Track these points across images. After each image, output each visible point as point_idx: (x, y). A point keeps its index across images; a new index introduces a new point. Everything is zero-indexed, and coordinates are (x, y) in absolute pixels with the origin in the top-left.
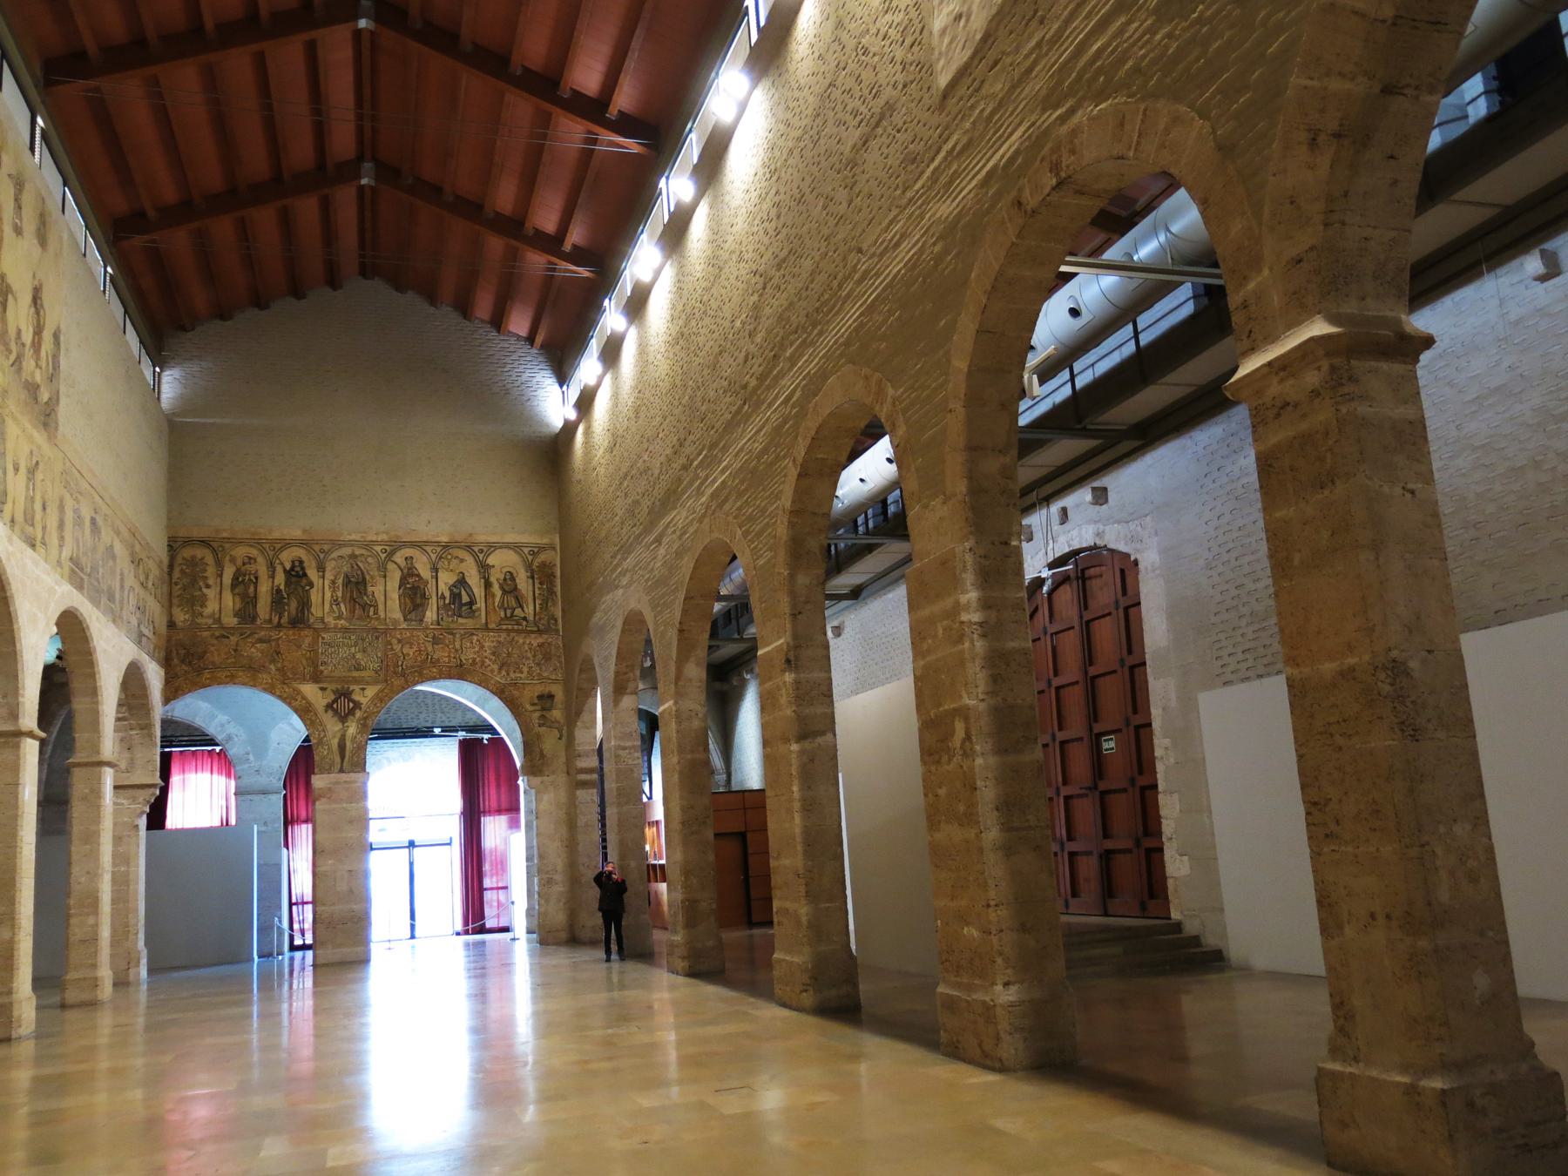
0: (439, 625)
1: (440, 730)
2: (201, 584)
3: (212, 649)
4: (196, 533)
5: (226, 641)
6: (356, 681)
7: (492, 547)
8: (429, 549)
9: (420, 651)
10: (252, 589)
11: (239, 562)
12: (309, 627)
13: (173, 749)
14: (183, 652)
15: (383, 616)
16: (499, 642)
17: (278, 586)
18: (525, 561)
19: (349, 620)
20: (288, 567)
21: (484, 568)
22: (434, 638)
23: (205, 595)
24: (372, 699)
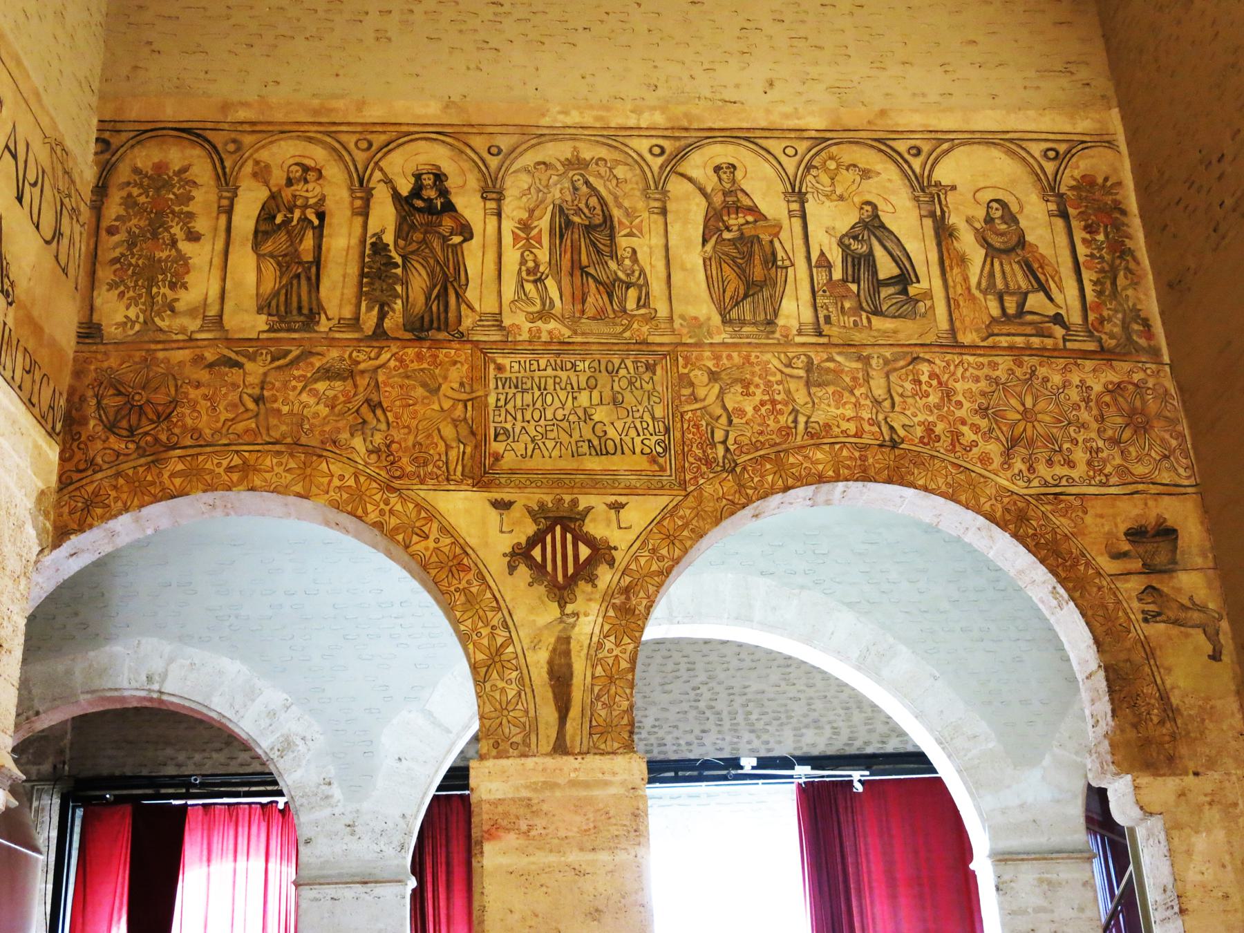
0: (820, 334)
1: (754, 762)
2: (176, 230)
3: (194, 393)
4: (172, 111)
5: (234, 375)
6: (594, 483)
7: (945, 143)
8: (776, 146)
9: (774, 402)
10: (308, 242)
11: (278, 177)
12: (462, 338)
13: (190, 802)
14: (112, 402)
15: (663, 311)
16: (996, 381)
17: (378, 236)
18: (1037, 175)
19: (572, 321)
20: (405, 188)
22: (809, 367)
23: (183, 260)
24: (643, 539)
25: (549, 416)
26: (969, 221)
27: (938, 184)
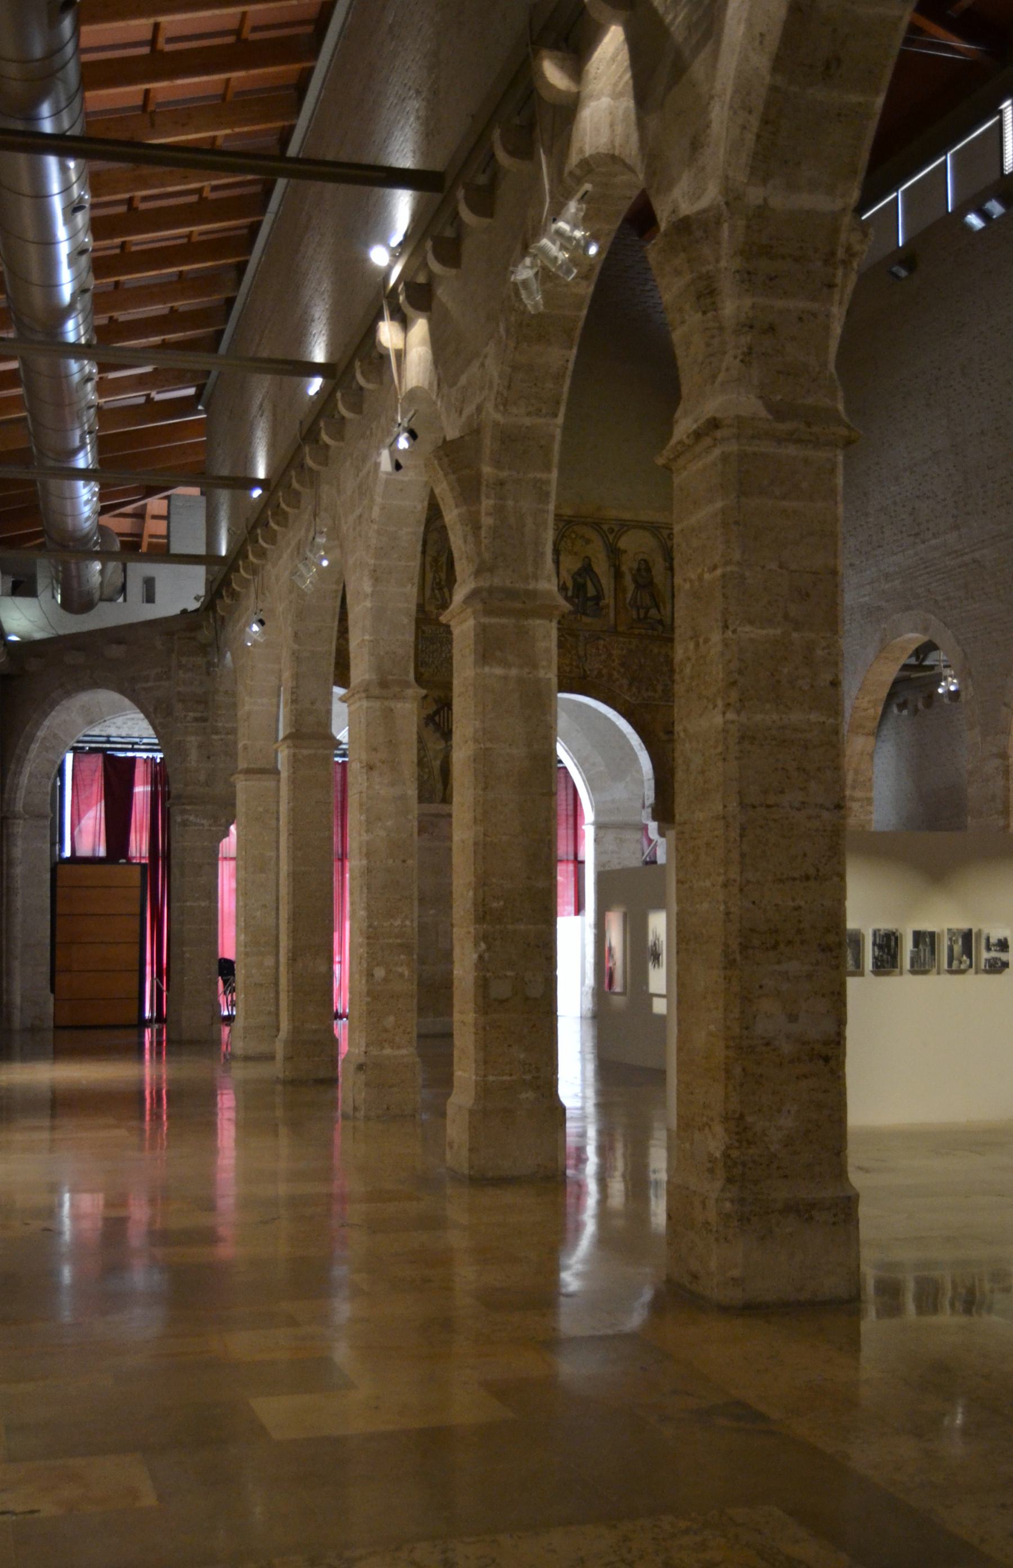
7: (625, 526)
21: (614, 553)
25: (444, 656)
26: (631, 569)
27: (619, 549)
